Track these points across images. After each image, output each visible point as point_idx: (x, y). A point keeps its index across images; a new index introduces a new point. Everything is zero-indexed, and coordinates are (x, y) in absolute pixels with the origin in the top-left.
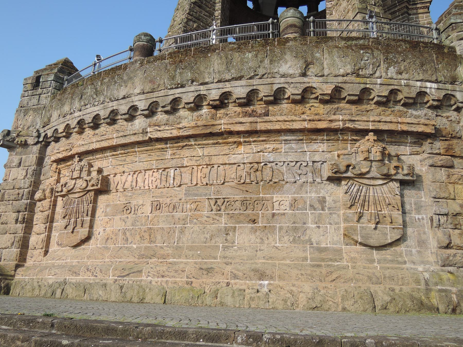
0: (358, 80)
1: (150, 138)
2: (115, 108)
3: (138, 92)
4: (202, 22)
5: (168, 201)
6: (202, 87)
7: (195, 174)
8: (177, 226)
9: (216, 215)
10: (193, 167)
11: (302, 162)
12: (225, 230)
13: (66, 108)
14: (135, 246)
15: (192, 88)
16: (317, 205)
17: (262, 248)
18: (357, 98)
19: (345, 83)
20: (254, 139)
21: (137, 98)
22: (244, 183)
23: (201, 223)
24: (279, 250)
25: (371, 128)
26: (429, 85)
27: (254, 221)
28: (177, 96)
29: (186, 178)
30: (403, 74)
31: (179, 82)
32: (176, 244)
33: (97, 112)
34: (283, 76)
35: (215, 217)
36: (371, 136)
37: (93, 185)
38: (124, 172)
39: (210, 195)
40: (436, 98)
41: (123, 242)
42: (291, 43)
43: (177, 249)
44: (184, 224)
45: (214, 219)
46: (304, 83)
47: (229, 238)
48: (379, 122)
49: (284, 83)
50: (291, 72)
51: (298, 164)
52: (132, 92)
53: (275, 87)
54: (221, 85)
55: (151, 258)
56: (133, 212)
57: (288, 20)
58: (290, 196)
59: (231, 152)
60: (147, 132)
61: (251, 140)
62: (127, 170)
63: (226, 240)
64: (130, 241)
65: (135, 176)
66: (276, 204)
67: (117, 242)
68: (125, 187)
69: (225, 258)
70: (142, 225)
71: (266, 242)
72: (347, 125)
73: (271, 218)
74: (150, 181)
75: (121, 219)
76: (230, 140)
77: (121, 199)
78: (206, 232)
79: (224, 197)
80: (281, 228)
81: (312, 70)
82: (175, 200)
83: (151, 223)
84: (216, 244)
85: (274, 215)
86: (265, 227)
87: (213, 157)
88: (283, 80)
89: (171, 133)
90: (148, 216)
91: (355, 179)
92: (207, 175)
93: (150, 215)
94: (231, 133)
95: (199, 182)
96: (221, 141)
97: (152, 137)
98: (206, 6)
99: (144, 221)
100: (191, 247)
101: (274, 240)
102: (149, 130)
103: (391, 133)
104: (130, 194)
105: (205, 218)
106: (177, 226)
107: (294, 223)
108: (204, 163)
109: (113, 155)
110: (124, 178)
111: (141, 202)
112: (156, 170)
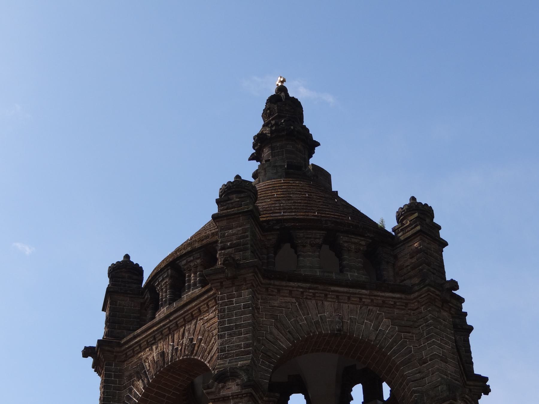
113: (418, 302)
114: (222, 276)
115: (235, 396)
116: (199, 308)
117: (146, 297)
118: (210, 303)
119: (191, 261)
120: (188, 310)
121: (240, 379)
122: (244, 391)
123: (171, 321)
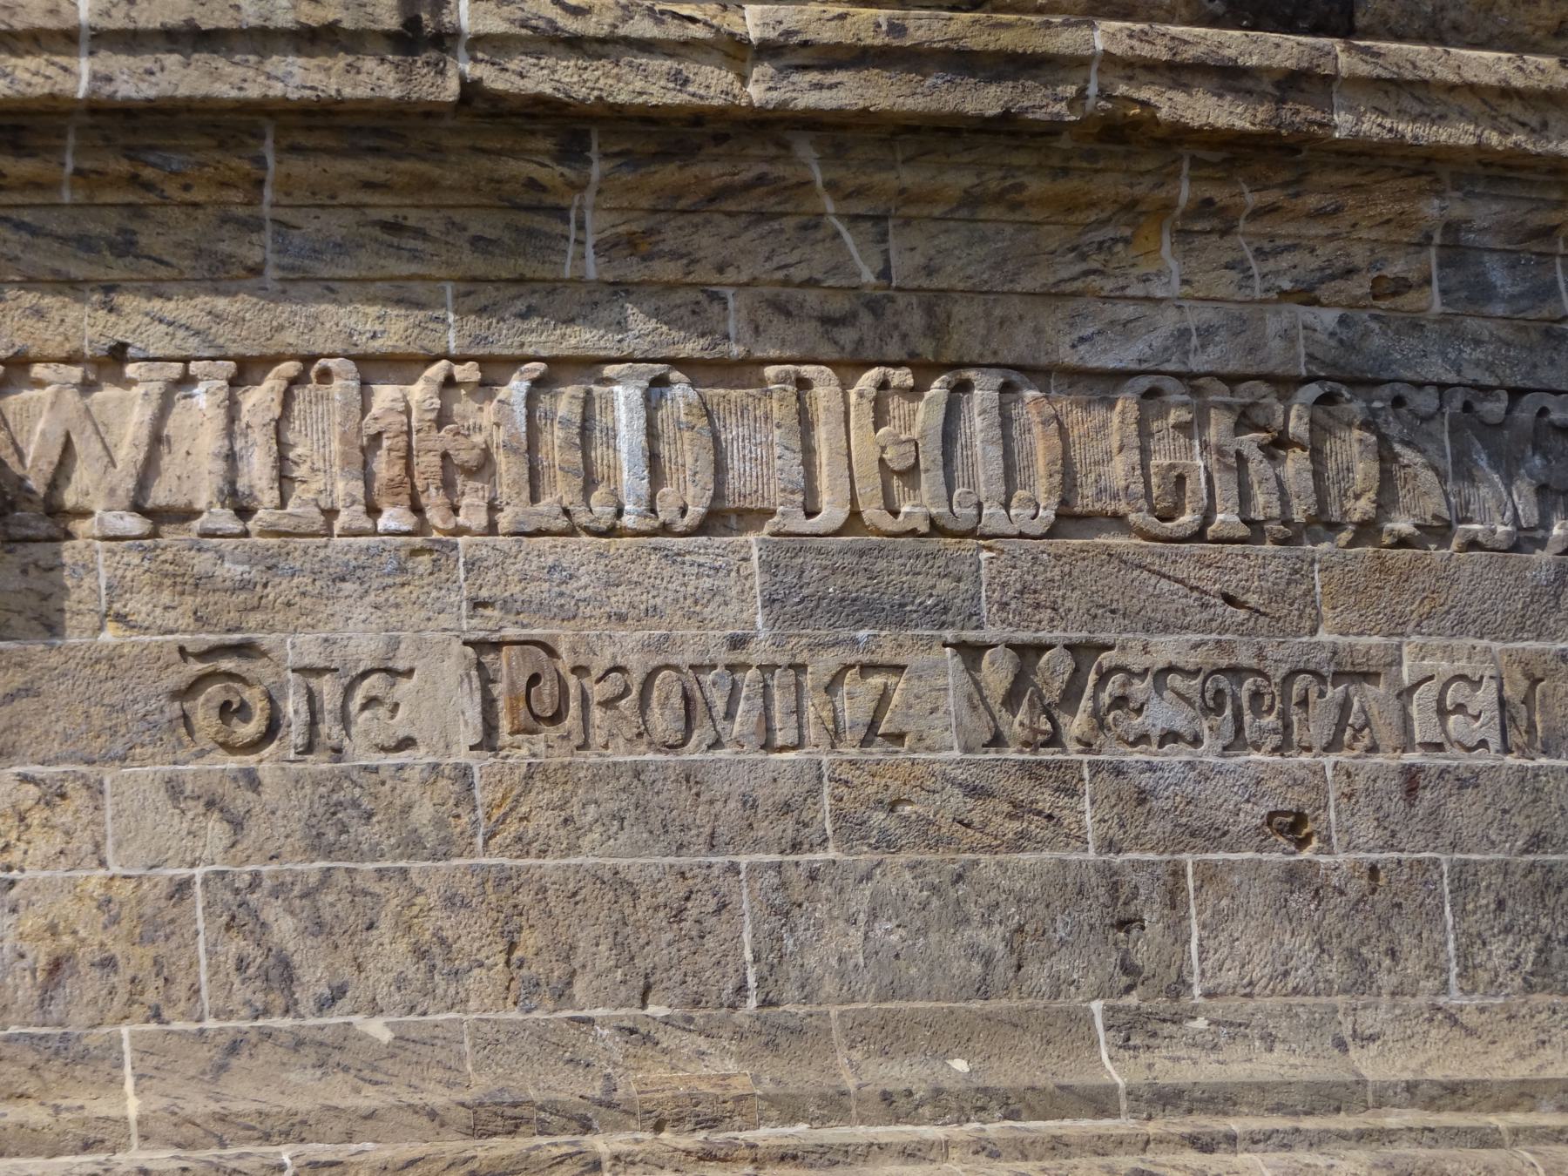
1: (470, 89)
5: (628, 646)
7: (823, 436)
8: (743, 860)
9: (1030, 771)
10: (808, 371)
11: (1550, 401)
12: (1114, 888)
14: (378, 1029)
17: (1370, 1021)
20: (1270, 197)
22: (1199, 536)
23: (927, 833)
24: (1470, 1032)
27: (1293, 827)
29: (761, 460)
32: (752, 1003)
35: (1024, 790)
38: (119, 354)
39: (972, 617)
41: (241, 992)
43: (772, 1045)
44: (796, 847)
47: (1142, 955)
51: (1525, 413)
55: (586, 1127)
59: (1096, 282)
60: (445, 40)
61: (1252, 199)
62: (155, 340)
63: (1127, 968)
64: (314, 977)
65: (260, 399)
66: (1421, 705)
67: (180, 990)
68: (160, 495)
69: (1167, 1099)
70: (412, 844)
71: (1386, 980)
73: (1396, 805)
74: (428, 464)
75: (174, 788)
76: (1110, 185)
77: (137, 606)
78: (975, 911)
79: (1077, 636)
80: (1464, 879)
82: (697, 642)
83: (513, 828)
84: (1061, 1003)
85: (1412, 780)
86: (1373, 871)
87: (960, 310)
90: (464, 772)
92: (931, 455)
95: (872, 512)
96: (1036, 186)
99: (423, 815)
100: (886, 1024)
101: (1434, 967)
104: (232, 570)
105: (956, 799)
106: (743, 860)
107: (1537, 842)
108: (894, 351)
110: (128, 409)
111: (364, 646)
112: (467, 372)
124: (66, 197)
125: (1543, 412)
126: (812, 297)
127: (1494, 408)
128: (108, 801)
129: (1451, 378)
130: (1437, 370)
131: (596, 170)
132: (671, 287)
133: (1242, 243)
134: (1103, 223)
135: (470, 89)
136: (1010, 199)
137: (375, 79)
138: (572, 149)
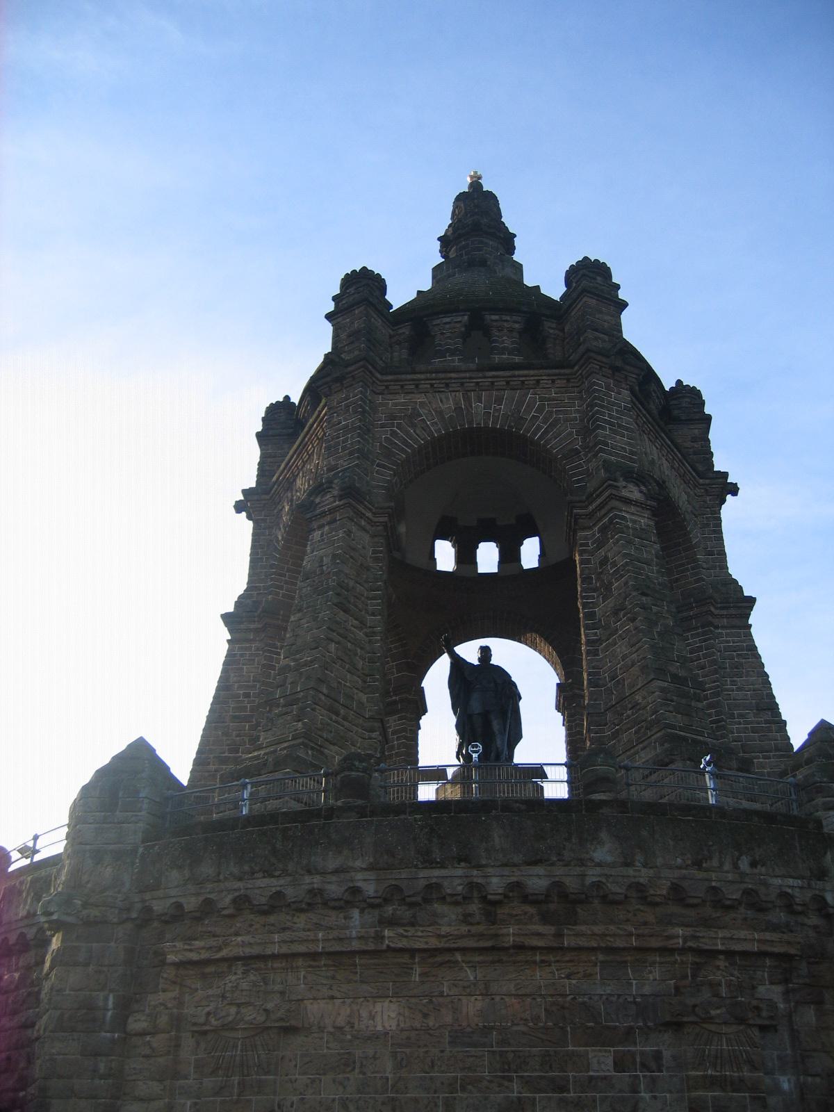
0: (701, 875)
1: (388, 946)
2: (315, 886)
3: (364, 866)
4: (362, 648)
6: (475, 872)
8: (441, 1096)
9: (503, 1077)
11: (627, 997)
13: (207, 869)
15: (459, 872)
16: (653, 1065)
18: (699, 901)
19: (684, 878)
20: (558, 958)
21: (359, 876)
25: (720, 947)
26: (791, 881)
28: (434, 880)
30: (759, 867)
31: (439, 860)
33: (278, 889)
34: (599, 865)
36: (721, 962)
37: (282, 1019)
40: (801, 903)
42: (605, 811)
45: (500, 1085)
46: (629, 876)
48: (731, 939)
49: (599, 876)
50: (609, 859)
51: (621, 1000)
52: (350, 864)
53: (589, 881)
54: (506, 871)
56: (357, 1071)
57: (597, 770)
58: (612, 1049)
60: (383, 937)
62: (338, 995)
72: (689, 944)
74: (385, 1017)
75: (334, 1081)
76: (521, 958)
81: (639, 858)
88: (598, 870)
89: (427, 943)
91: (704, 1025)
93: (390, 1076)
94: (520, 948)
97: (392, 945)
98: (356, 606)
102: (386, 933)
103: (744, 954)
106: (441, 1096)
109: (310, 966)
113: (706, 490)
114: (604, 360)
115: (636, 503)
116: (538, 381)
117: (401, 331)
118: (559, 381)
119: (507, 321)
120: (519, 376)
121: (645, 486)
122: (649, 502)
123: (485, 377)
124: (324, 969)
125: (626, 999)
126: (461, 982)
127: (614, 999)
128: (323, 1083)
129: (603, 993)
130: (600, 991)
131: (417, 960)
132: (433, 982)
133: (553, 968)
134: (522, 966)
135: (388, 946)
136: (500, 961)
137: (371, 947)
138: (413, 957)
